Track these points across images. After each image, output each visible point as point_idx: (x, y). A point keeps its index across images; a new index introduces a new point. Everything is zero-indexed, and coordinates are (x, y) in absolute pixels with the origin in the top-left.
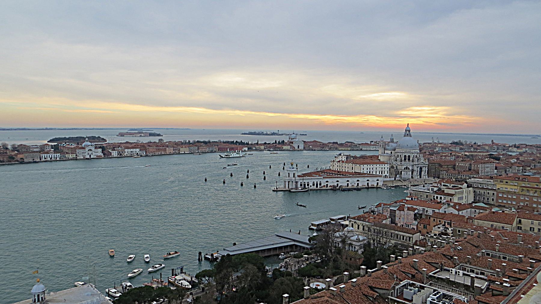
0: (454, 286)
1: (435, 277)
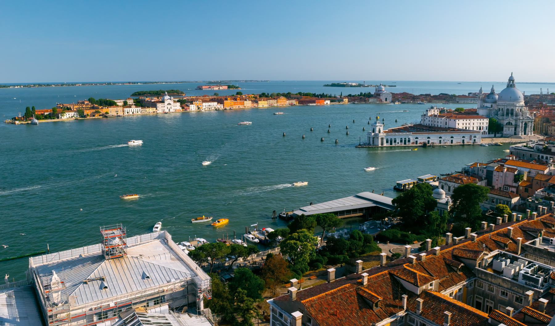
0: (553, 258)
1: (532, 247)
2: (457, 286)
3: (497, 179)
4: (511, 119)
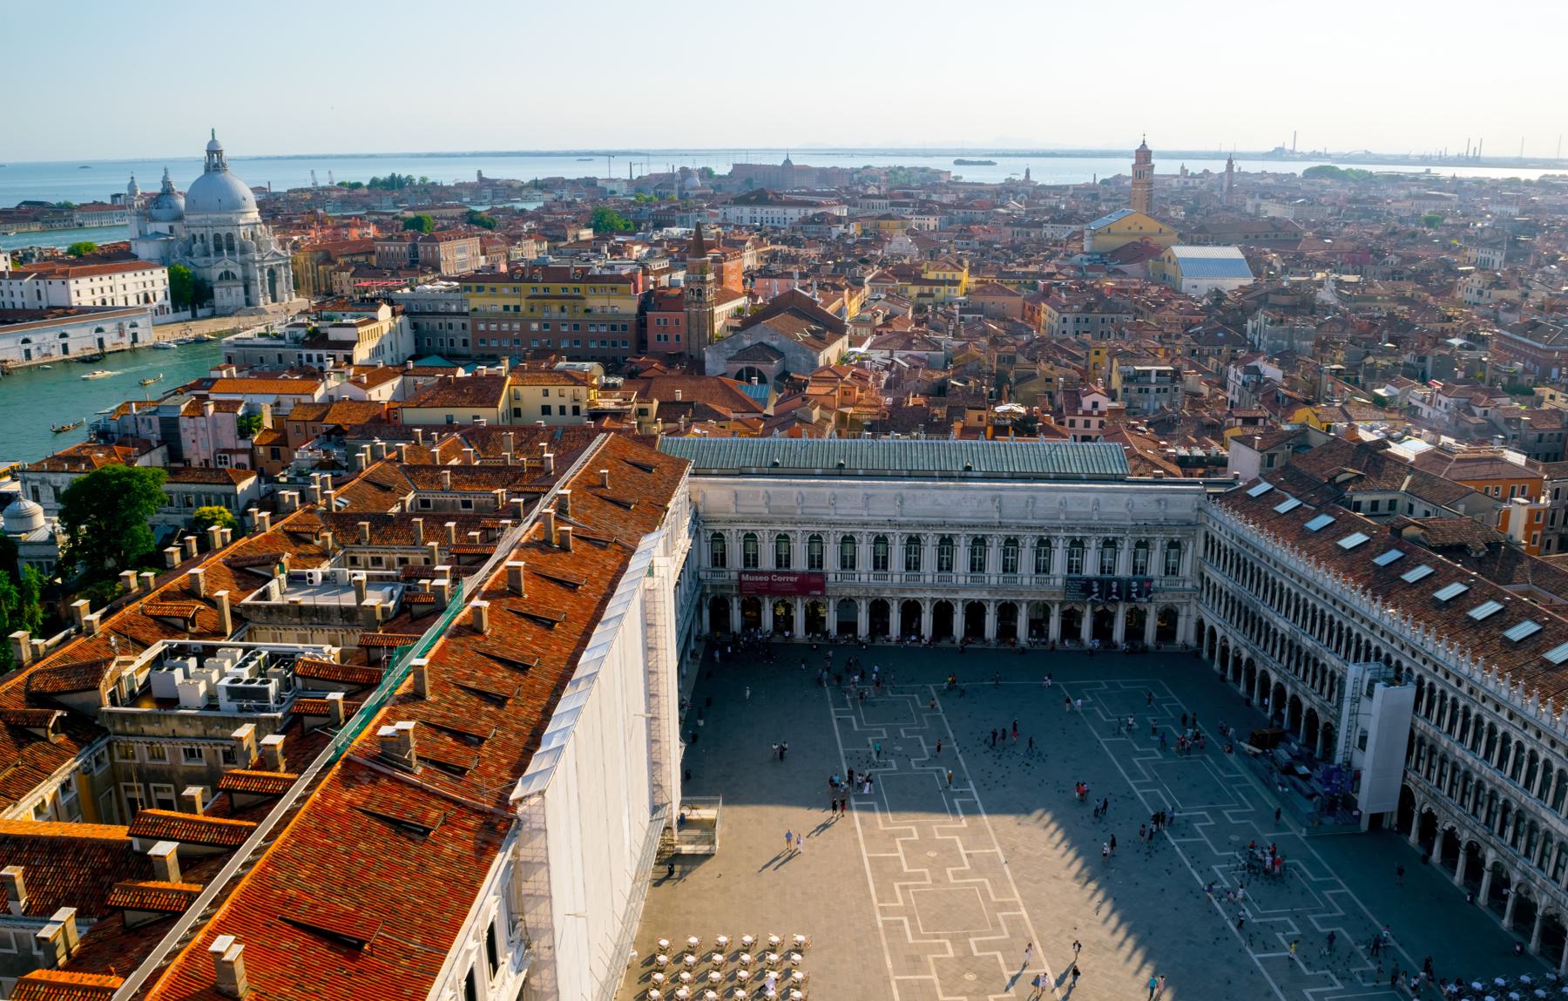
1: (258, 607)
2: (54, 781)
3: (193, 437)
4: (230, 263)
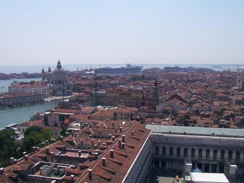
4: (60, 86)
